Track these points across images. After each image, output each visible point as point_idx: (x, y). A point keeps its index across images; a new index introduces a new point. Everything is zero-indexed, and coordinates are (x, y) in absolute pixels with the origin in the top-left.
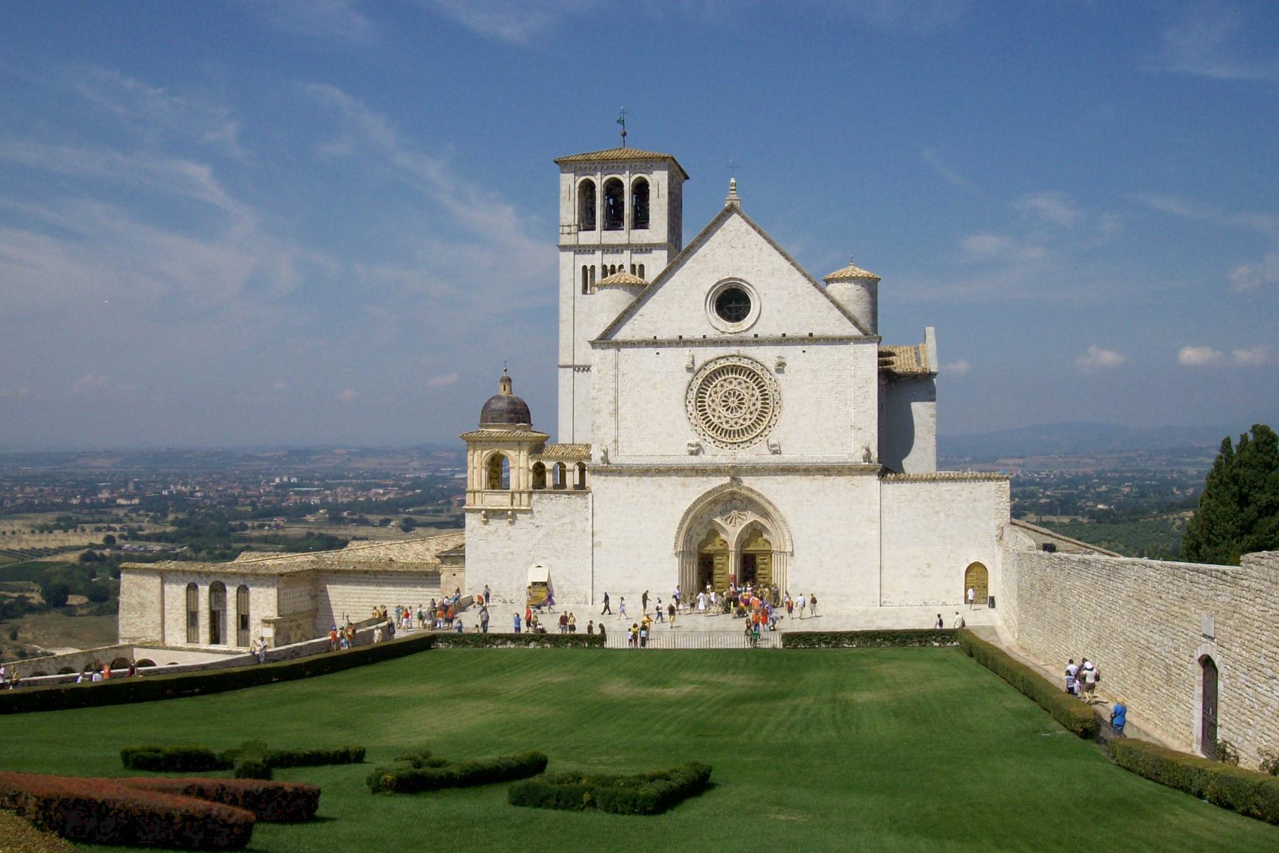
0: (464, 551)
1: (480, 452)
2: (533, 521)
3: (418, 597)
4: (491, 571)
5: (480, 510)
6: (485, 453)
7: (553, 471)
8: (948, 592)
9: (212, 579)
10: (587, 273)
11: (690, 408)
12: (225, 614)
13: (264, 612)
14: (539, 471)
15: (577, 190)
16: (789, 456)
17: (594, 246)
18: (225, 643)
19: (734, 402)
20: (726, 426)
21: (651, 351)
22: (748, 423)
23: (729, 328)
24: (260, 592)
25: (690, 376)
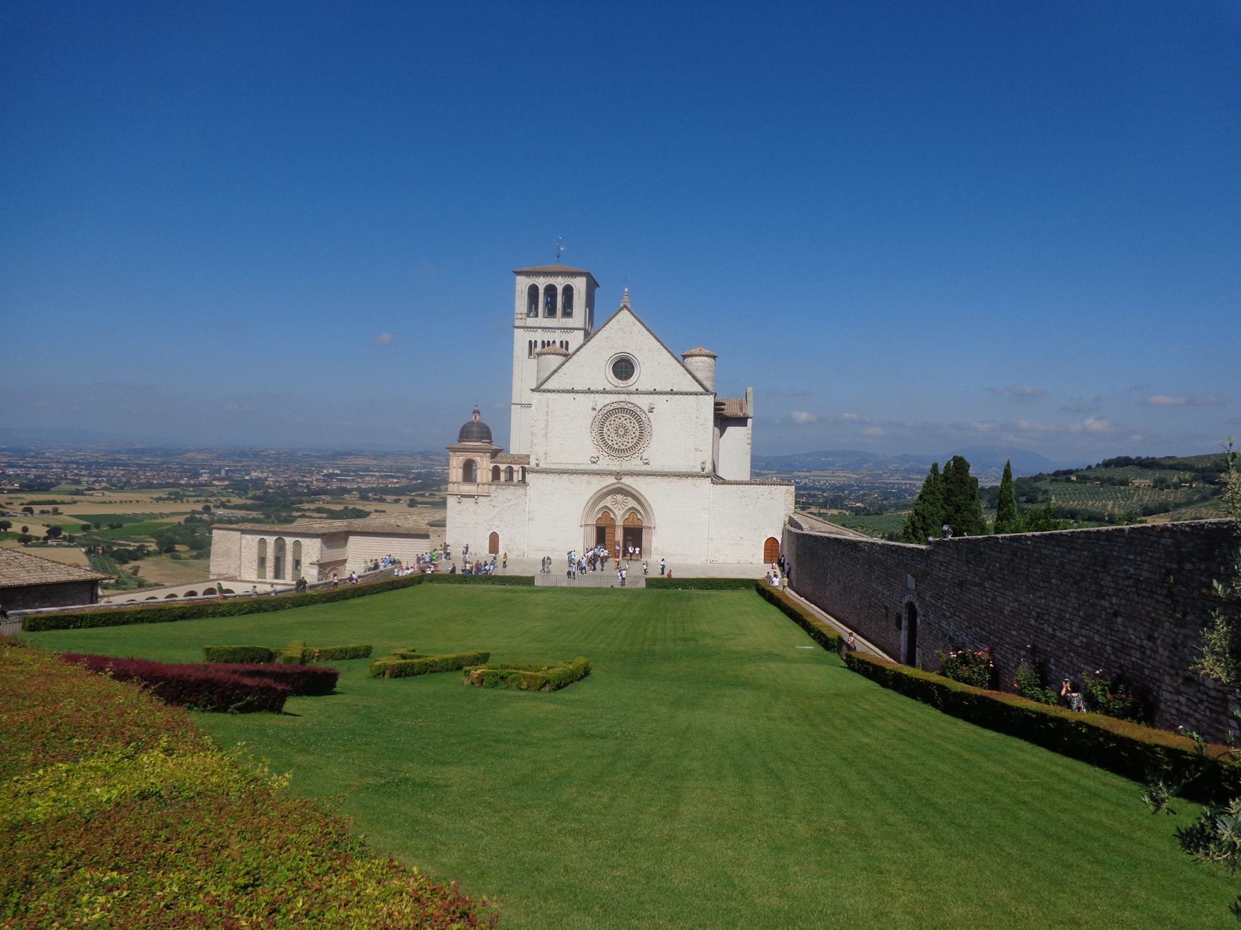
0: (445, 521)
5: (457, 495)
6: (461, 458)
7: (505, 471)
8: (753, 556)
10: (532, 345)
11: (594, 434)
12: (284, 560)
14: (496, 472)
15: (527, 291)
16: (654, 467)
17: (536, 328)
18: (284, 578)
19: (622, 431)
20: (616, 446)
21: (572, 395)
22: (630, 445)
23: (621, 383)
25: (595, 412)
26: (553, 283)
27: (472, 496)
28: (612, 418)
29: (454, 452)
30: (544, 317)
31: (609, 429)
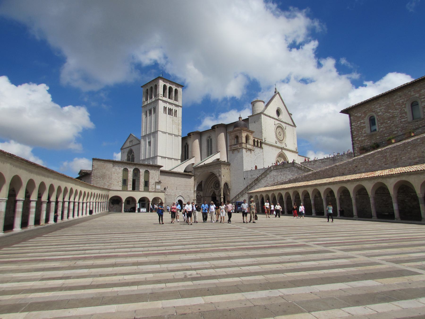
2: (255, 154)
3: (179, 182)
9: (134, 167)
10: (165, 108)
13: (155, 180)
16: (287, 148)
20: (279, 139)
22: (282, 139)
25: (275, 126)
28: (278, 129)
29: (244, 130)
31: (278, 132)
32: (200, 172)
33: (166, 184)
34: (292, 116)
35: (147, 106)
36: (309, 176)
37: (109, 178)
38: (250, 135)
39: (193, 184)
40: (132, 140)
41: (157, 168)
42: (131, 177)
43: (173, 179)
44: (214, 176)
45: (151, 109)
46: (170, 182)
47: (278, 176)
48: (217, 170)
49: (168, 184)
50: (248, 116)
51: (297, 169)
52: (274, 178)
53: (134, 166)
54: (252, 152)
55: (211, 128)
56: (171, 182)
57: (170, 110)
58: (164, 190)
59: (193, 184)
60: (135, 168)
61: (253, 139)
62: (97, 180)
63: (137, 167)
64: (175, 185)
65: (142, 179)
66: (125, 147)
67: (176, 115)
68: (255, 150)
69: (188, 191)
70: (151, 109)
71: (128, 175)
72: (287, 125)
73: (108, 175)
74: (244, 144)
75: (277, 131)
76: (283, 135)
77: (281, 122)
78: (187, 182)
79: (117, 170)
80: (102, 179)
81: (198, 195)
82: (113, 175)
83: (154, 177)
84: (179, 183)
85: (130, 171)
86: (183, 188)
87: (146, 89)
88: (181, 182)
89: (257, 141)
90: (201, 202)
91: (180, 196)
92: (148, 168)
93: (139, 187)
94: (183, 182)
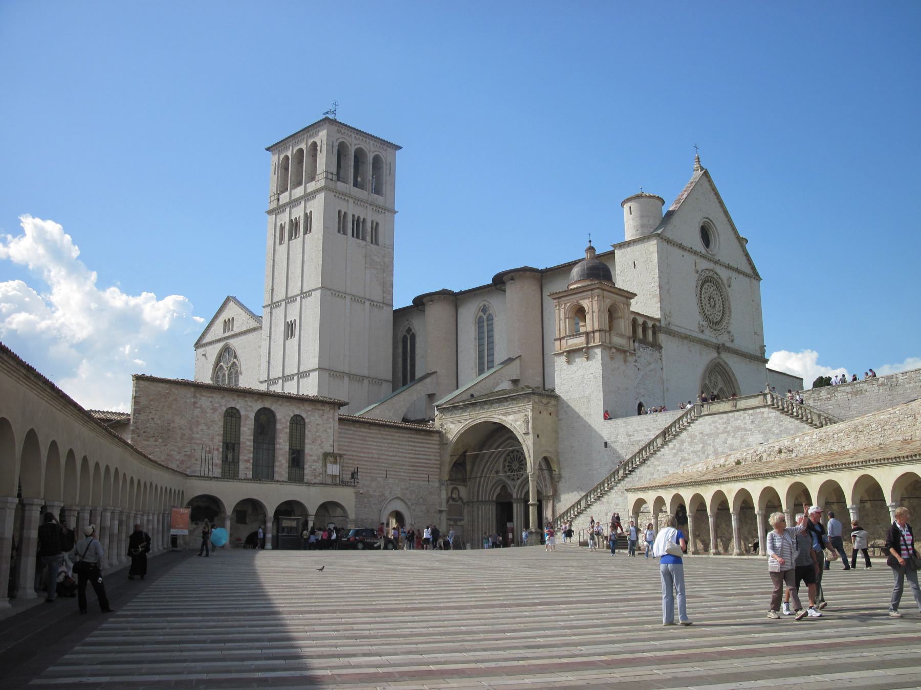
1: (563, 306)
4: (616, 402)
9: (258, 406)
10: (342, 217)
13: (322, 448)
20: (711, 317)
22: (719, 318)
24: (317, 424)
26: (362, 147)
27: (625, 352)
28: (706, 286)
30: (356, 184)
32: (459, 422)
33: (354, 460)
34: (748, 247)
35: (284, 211)
36: (836, 436)
37: (182, 439)
38: (622, 305)
39: (436, 462)
40: (233, 318)
41: (328, 409)
42: (249, 438)
43: (375, 444)
44: (507, 436)
45: (296, 218)
46: (364, 453)
47: (717, 434)
48: (517, 416)
49: (359, 460)
50: (612, 246)
51: (778, 413)
52: (705, 444)
53: (256, 400)
54: (631, 359)
55: (490, 282)
56: (370, 455)
57: (358, 224)
58: (352, 480)
59: (436, 460)
60: (262, 407)
61: (632, 316)
62: (145, 443)
63: (267, 404)
64: (382, 463)
65: (284, 442)
66: (207, 339)
67: (375, 241)
68: (638, 353)
69: (421, 483)
70: (296, 218)
71: (240, 429)
72: (734, 275)
73: (181, 428)
74: (603, 333)
75: (703, 291)
76: (722, 306)
77: (716, 262)
78: (418, 454)
79: (208, 415)
80: (160, 440)
81: (454, 496)
82: (195, 430)
83: (320, 437)
84: (393, 458)
85: (247, 417)
86: (405, 474)
87: (282, 156)
88: (400, 454)
89: (644, 323)
90: (461, 520)
91: (398, 498)
92: (302, 408)
93: (273, 467)
94: (406, 455)
